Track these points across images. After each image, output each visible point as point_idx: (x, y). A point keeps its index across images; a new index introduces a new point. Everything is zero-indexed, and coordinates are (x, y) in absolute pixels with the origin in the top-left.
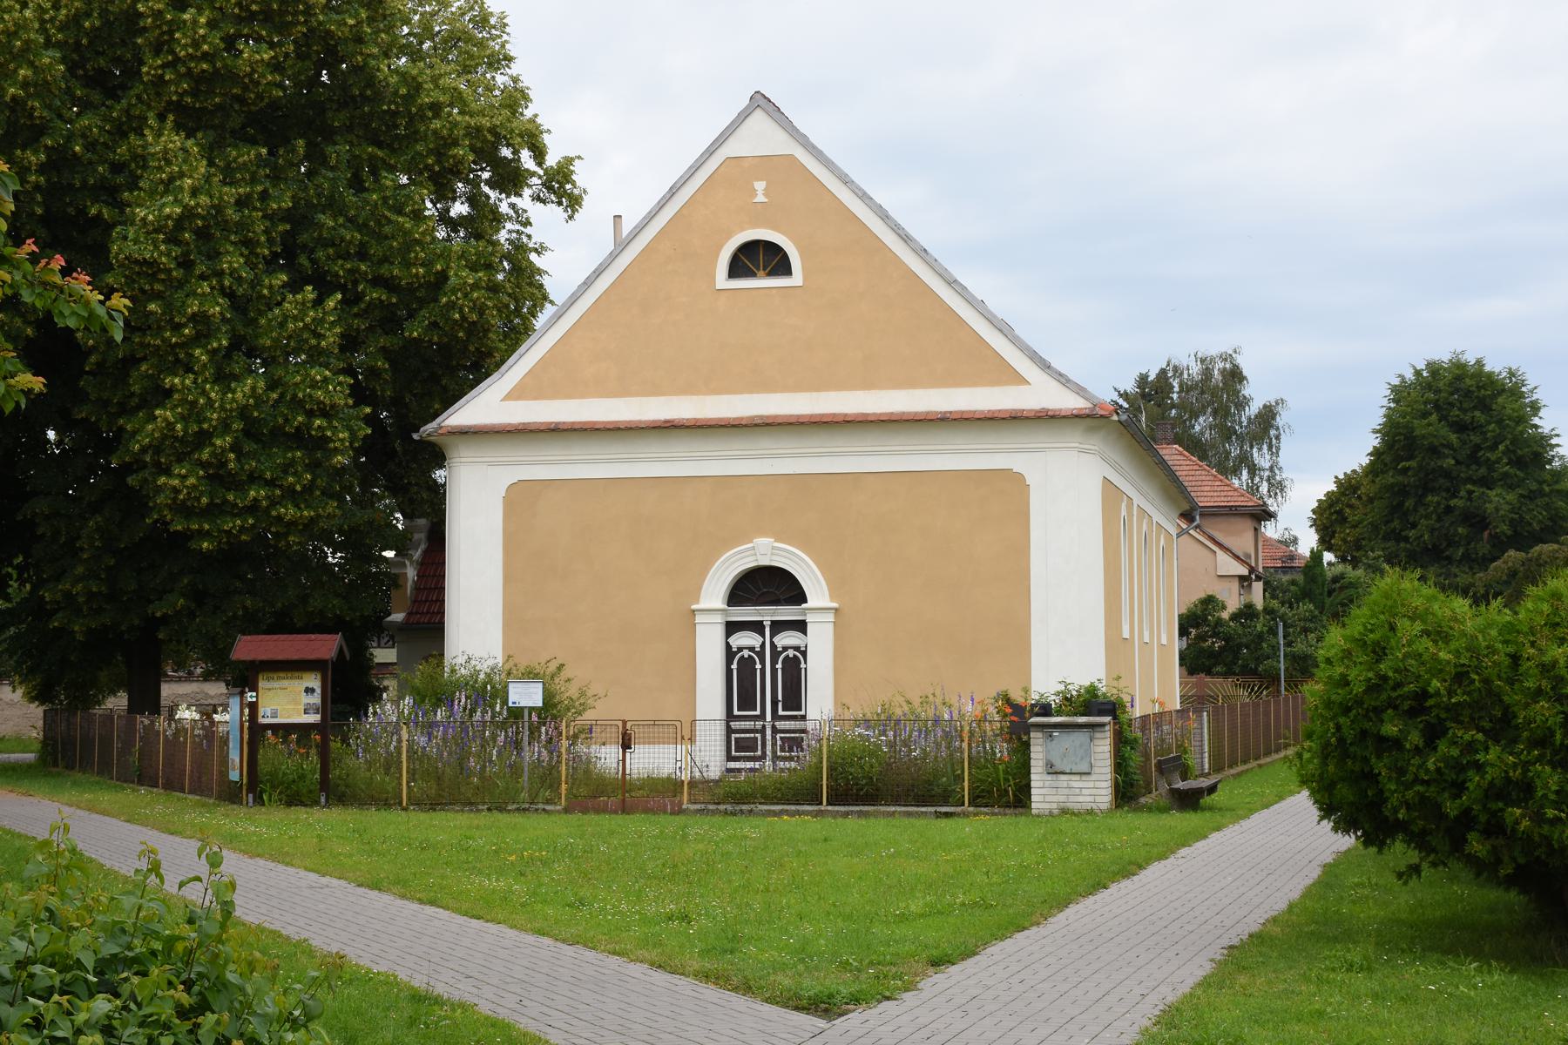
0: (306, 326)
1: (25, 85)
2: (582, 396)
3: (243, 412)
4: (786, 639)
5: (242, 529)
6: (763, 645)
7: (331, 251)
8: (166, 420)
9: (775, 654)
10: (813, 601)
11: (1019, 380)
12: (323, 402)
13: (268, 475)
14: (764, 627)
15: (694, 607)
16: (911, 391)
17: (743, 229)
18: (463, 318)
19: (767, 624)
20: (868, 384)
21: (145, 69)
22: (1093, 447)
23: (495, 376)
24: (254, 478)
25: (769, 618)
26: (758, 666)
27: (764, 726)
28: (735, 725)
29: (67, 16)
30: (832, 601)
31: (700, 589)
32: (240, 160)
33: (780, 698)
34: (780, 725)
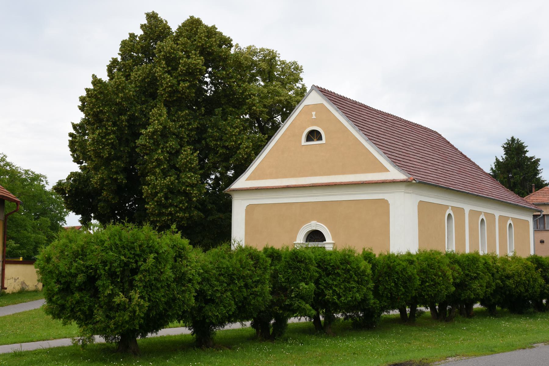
0: (187, 161)
1: (122, 98)
2: (266, 179)
3: (168, 187)
5: (168, 220)
7: (211, 139)
8: (146, 189)
10: (327, 241)
11: (387, 170)
12: (189, 183)
13: (175, 204)
15: (295, 242)
17: (309, 127)
18: (243, 156)
20: (343, 173)
21: (158, 91)
22: (410, 191)
24: (171, 205)
29: (142, 78)
32: (181, 115)
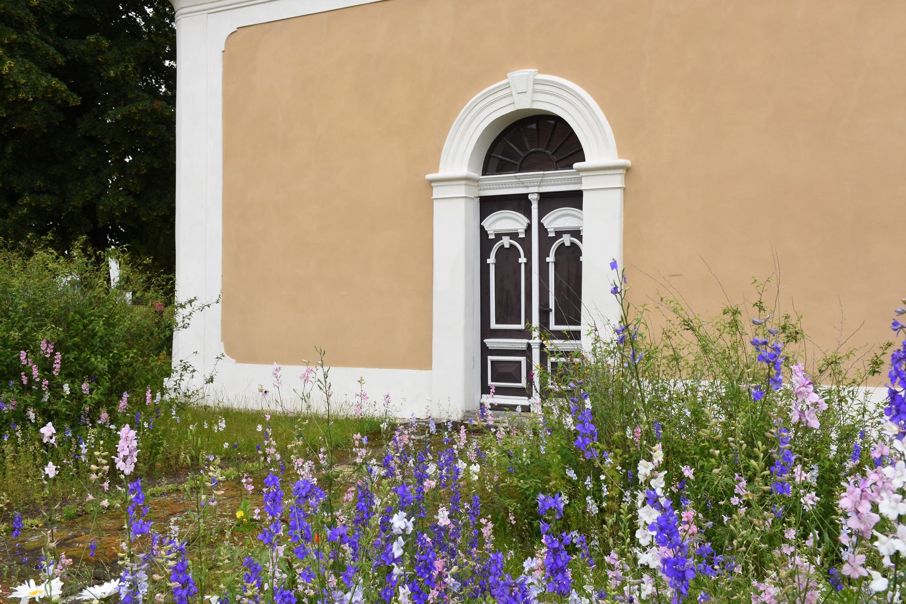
6: (528, 230)
9: (546, 241)
14: (530, 203)
15: (430, 176)
19: (533, 198)
25: (536, 190)
26: (522, 260)
27: (529, 346)
28: (492, 343)
30: (620, 157)
33: (552, 305)
34: (551, 344)
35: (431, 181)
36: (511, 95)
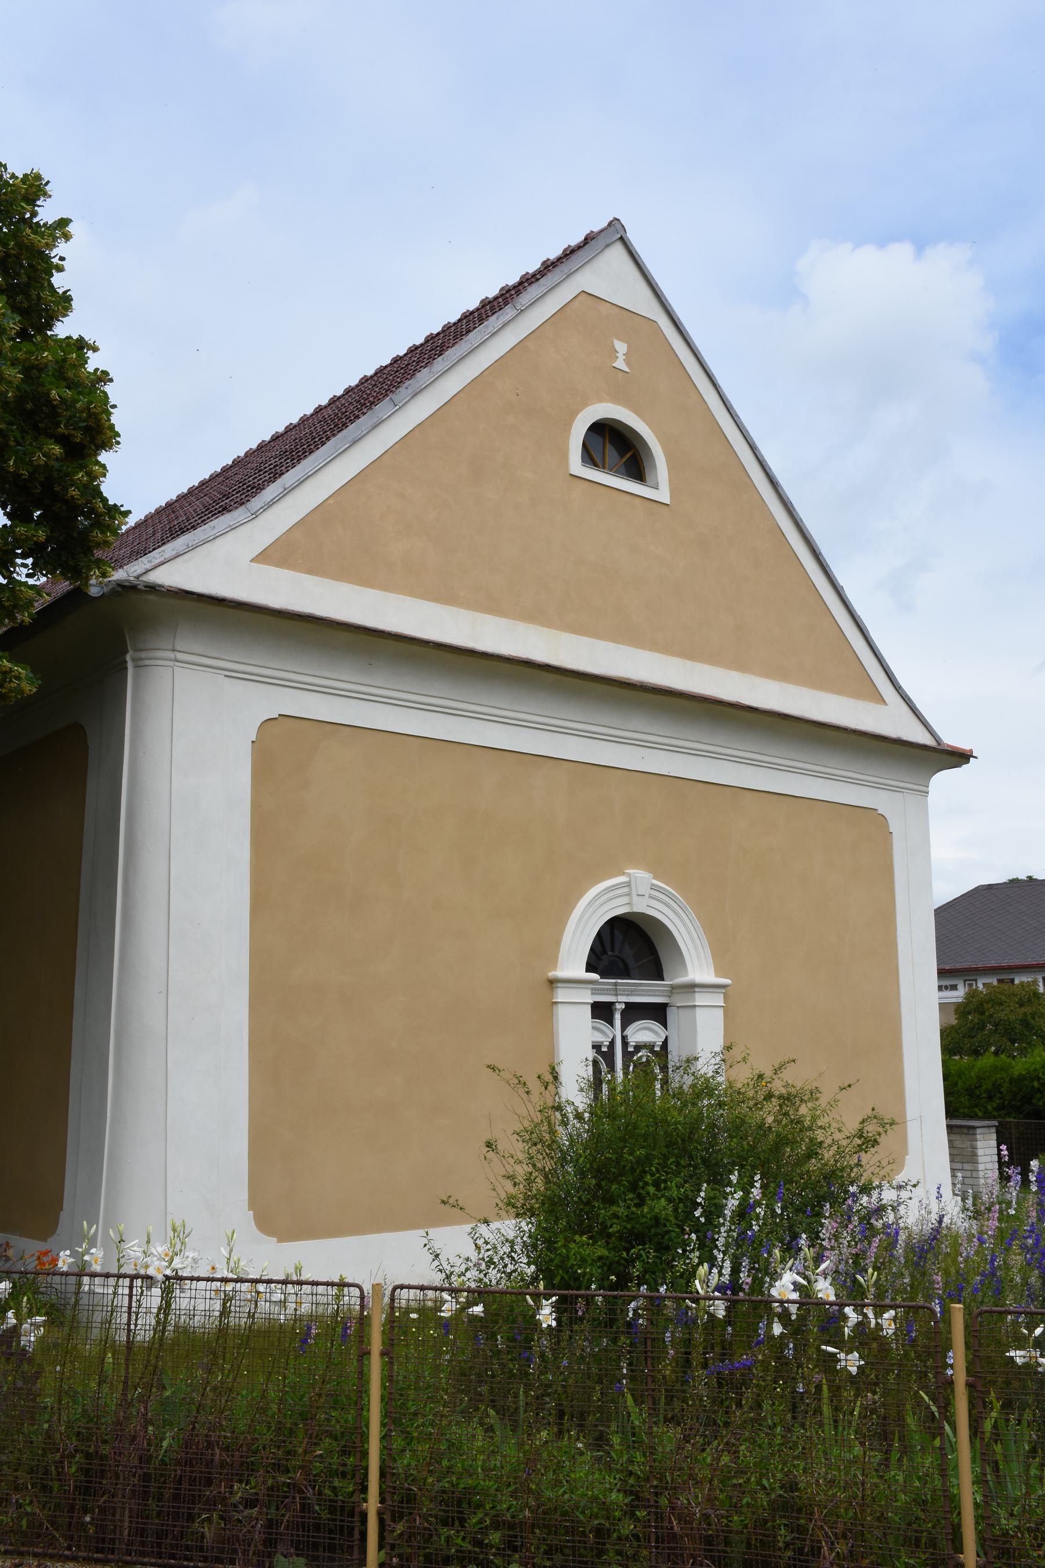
2: (385, 587)
4: (643, 1033)
6: (612, 1043)
16: (784, 684)
20: (740, 664)
23: (239, 514)
31: (557, 944)
35: (553, 982)
36: (629, 894)
